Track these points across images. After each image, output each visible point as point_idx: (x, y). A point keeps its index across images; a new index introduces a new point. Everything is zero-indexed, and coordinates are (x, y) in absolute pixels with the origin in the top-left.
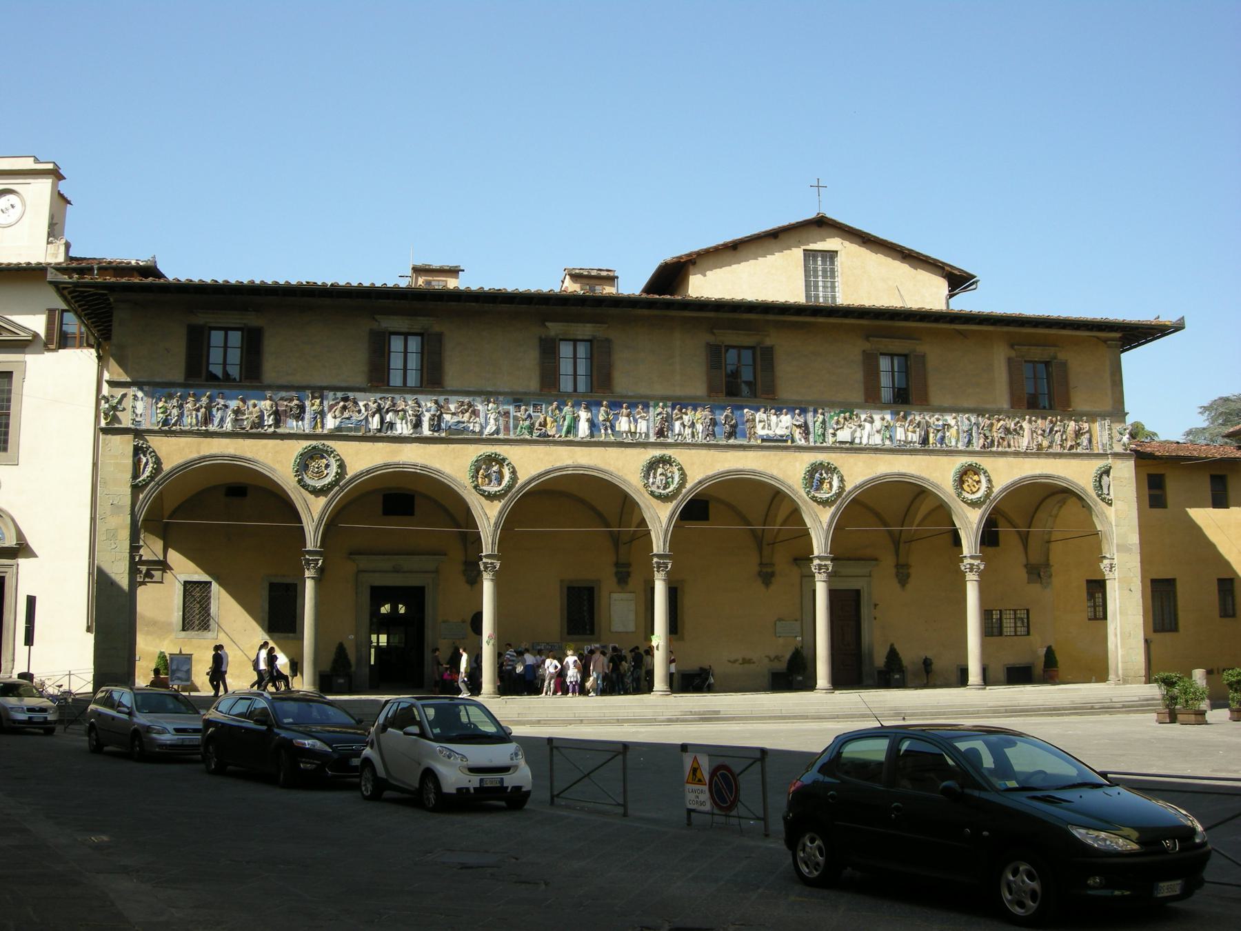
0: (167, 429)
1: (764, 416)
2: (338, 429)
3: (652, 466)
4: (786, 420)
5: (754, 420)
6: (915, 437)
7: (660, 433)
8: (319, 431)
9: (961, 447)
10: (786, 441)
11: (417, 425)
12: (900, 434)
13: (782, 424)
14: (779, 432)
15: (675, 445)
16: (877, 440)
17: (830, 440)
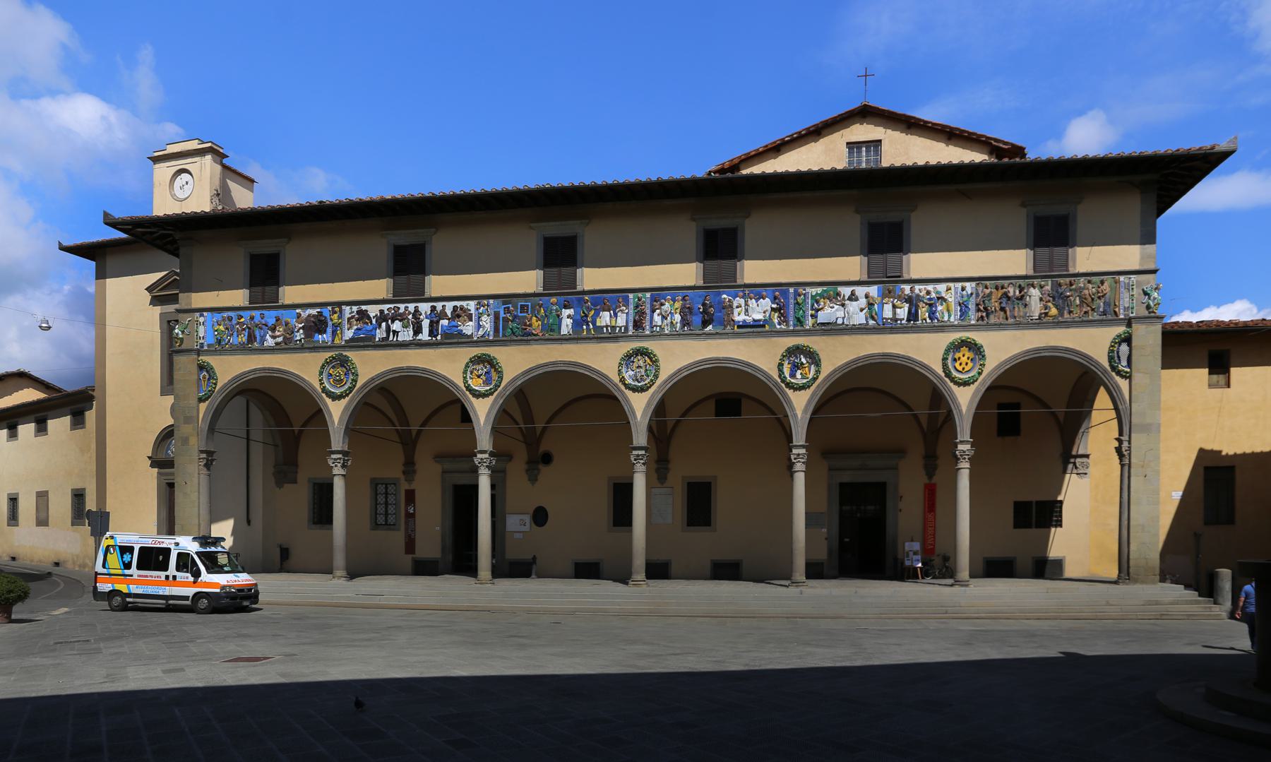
0: (220, 347)
1: (742, 301)
2: (352, 340)
3: (628, 358)
4: (767, 303)
5: (731, 306)
6: (903, 313)
7: (638, 325)
8: (337, 341)
9: (954, 319)
10: (763, 326)
11: (418, 330)
12: (888, 312)
13: (759, 309)
14: (759, 316)
15: (653, 336)
16: (860, 319)
17: (810, 322)
